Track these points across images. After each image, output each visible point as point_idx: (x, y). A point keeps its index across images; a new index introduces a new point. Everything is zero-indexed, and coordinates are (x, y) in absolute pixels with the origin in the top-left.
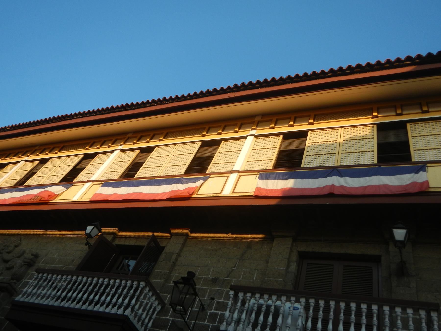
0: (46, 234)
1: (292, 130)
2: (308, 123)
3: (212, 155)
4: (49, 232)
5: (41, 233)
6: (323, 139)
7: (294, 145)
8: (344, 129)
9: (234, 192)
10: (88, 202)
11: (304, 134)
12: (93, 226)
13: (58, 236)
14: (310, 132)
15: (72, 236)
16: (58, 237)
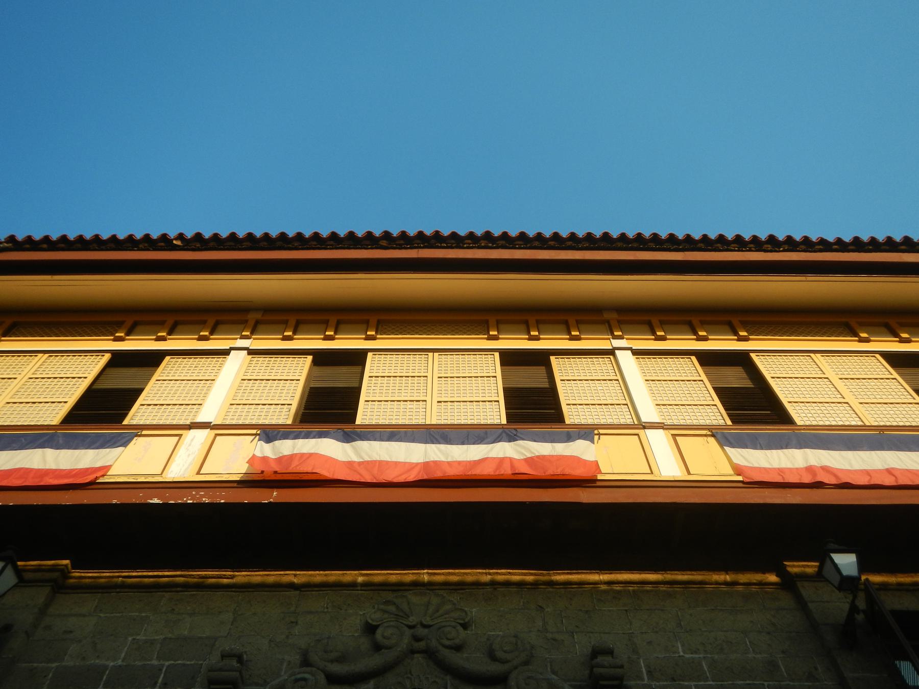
0: (551, 584)
1: (363, 346)
2: (322, 337)
3: (356, 385)
4: (561, 577)
5: (530, 578)
6: (398, 372)
7: (337, 377)
8: (373, 354)
9: (201, 473)
10: (235, 485)
11: (357, 358)
12: (831, 554)
13: (603, 587)
14: (370, 355)
15: (663, 588)
16: (605, 591)
